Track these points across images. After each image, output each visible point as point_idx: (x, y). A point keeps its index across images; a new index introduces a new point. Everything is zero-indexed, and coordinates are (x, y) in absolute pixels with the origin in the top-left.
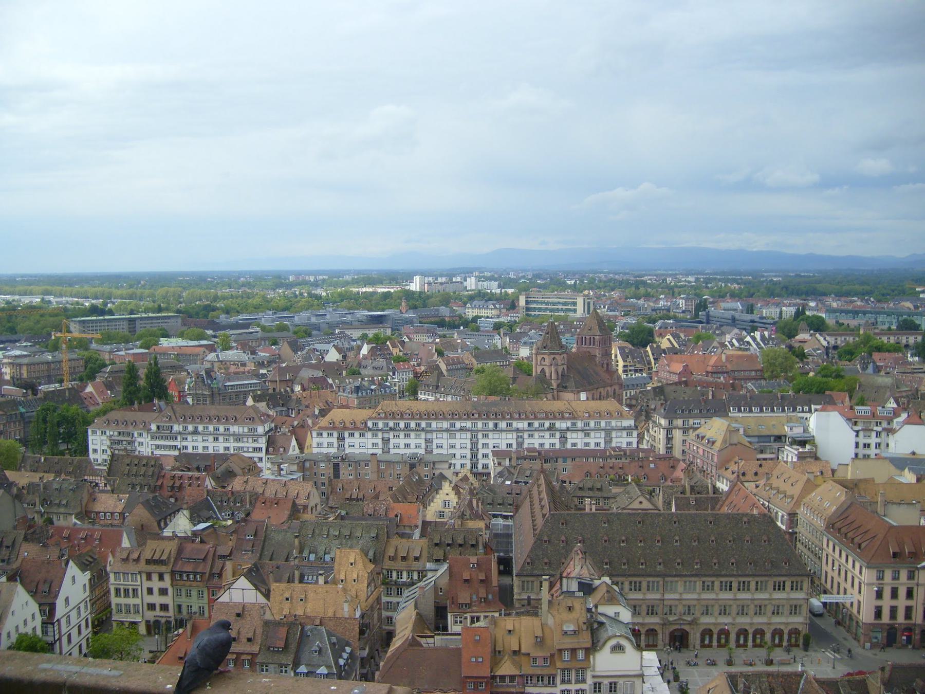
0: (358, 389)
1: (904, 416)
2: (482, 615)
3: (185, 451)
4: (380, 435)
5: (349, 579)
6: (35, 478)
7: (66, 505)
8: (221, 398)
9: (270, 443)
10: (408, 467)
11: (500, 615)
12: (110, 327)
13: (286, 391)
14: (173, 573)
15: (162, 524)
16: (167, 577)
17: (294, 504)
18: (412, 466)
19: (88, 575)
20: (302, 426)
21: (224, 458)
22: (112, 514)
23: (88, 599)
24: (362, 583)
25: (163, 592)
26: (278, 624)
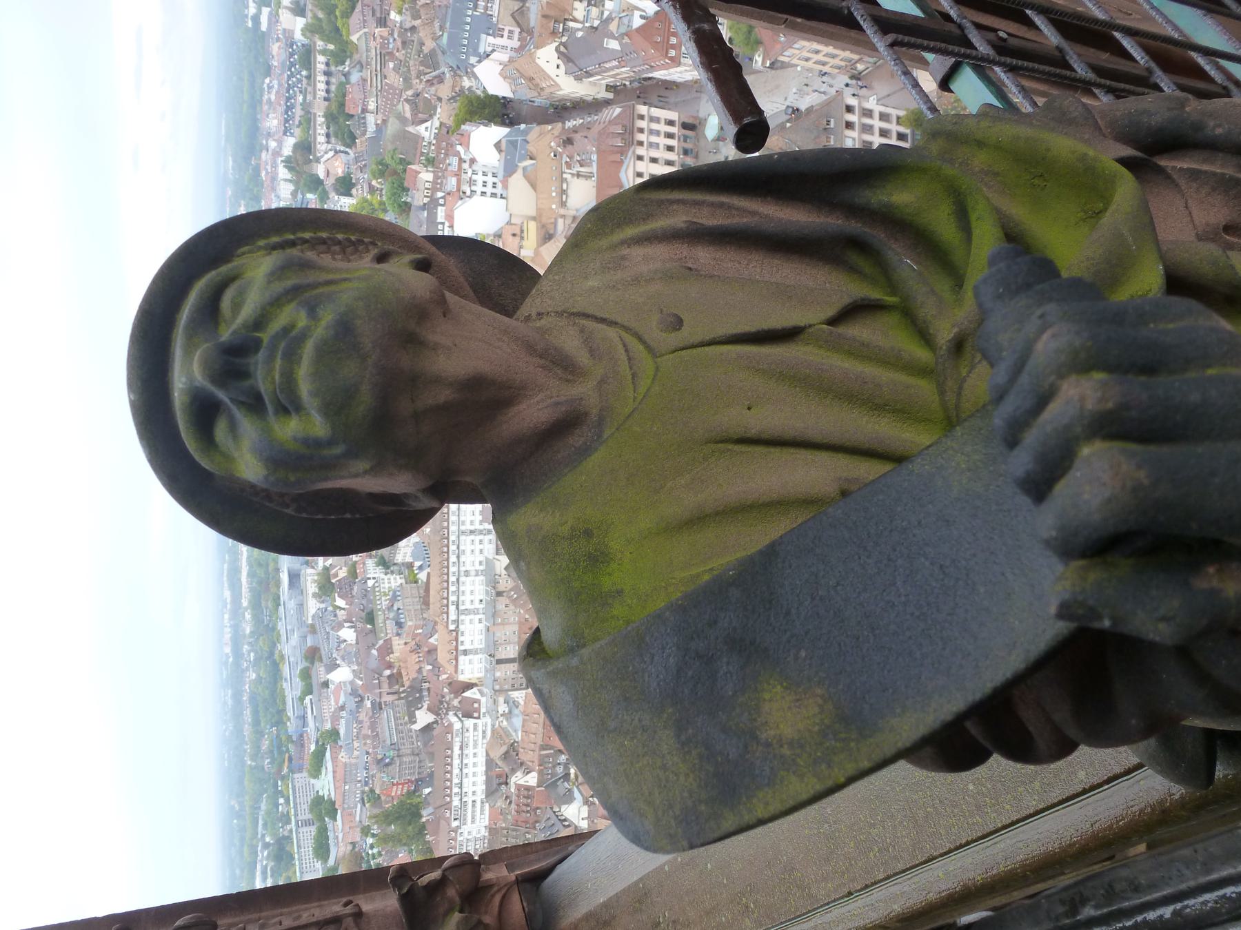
1: (459, 148)
8: (403, 747)
9: (468, 715)
10: (500, 598)
12: (306, 846)
15: (566, 823)
18: (499, 594)
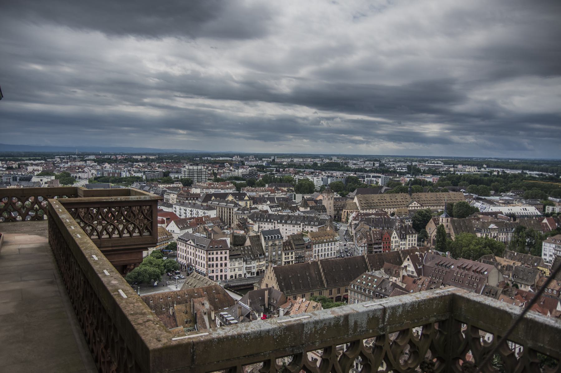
6: (511, 263)
7: (527, 280)
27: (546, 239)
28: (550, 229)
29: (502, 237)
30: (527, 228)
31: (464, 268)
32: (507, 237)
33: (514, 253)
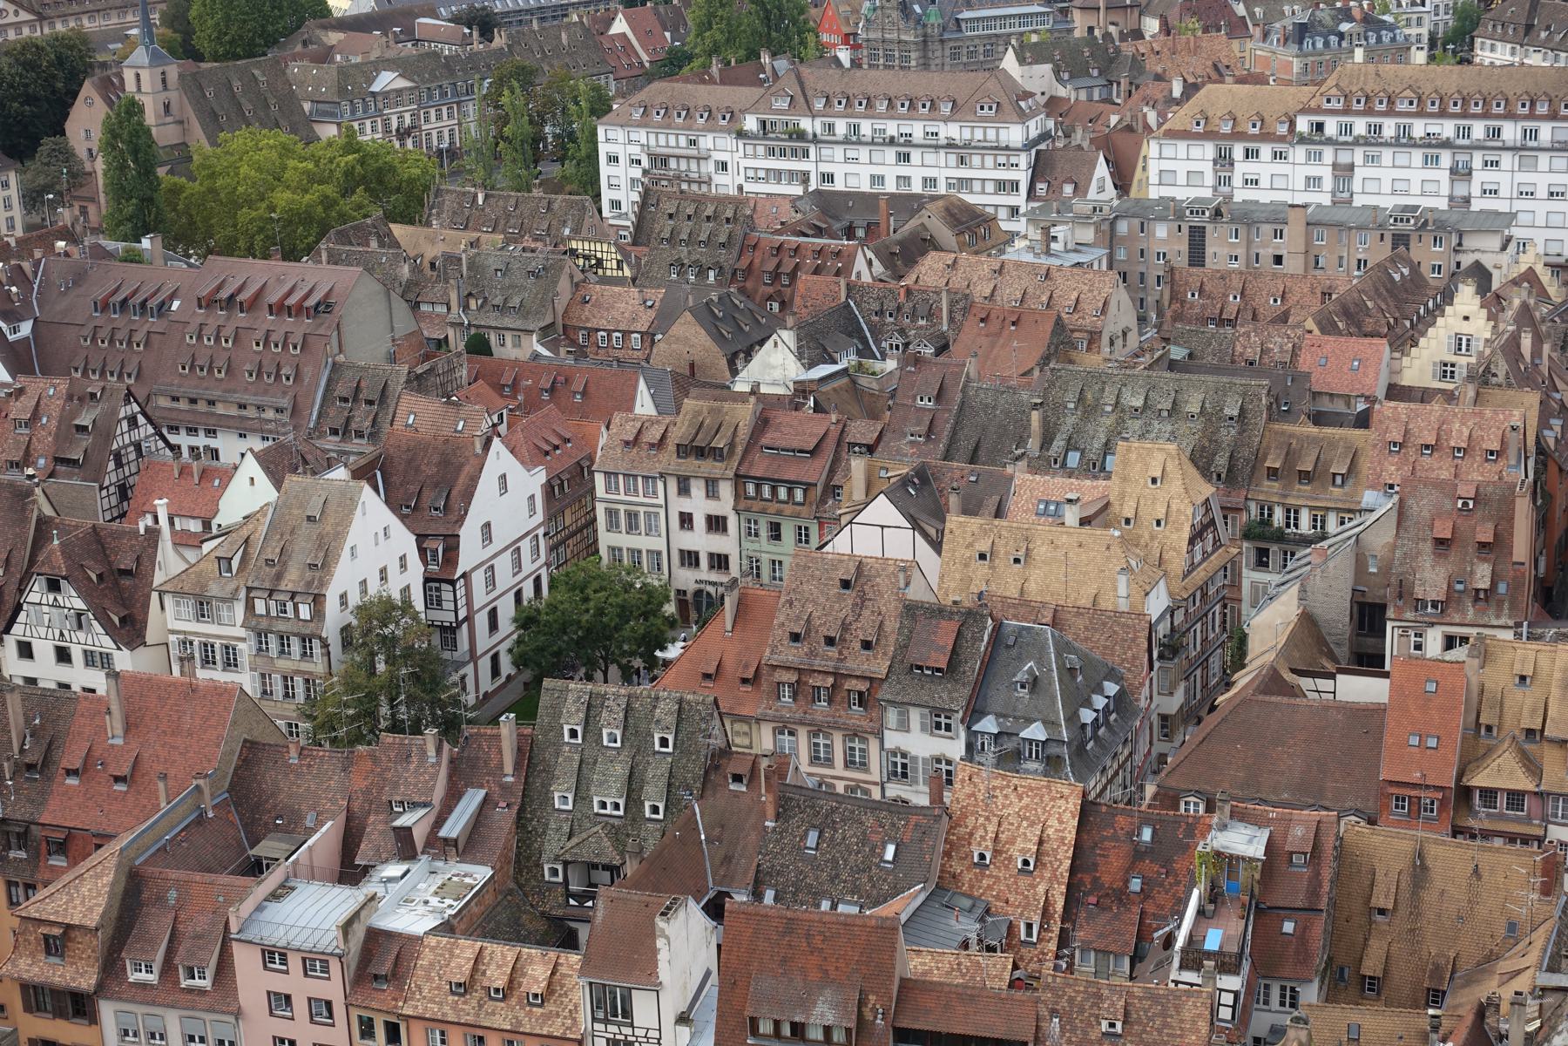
0: (1302, 32)
2: (1473, 631)
3: (827, 187)
4: (1328, 154)
5: (1148, 518)
6: (459, 242)
7: (522, 311)
8: (948, 52)
9: (1039, 170)
11: (1518, 635)
13: (1107, 36)
14: (739, 479)
16: (726, 490)
17: (1059, 322)
18: (1400, 240)
19: (540, 476)
20: (1130, 129)
21: (906, 204)
22: (626, 334)
23: (541, 531)
24: (1178, 530)
25: (716, 524)
26: (937, 612)
27: (610, 109)
28: (641, 63)
29: (439, 127)
30: (546, 68)
31: (279, 309)
32: (460, 124)
33: (475, 196)
